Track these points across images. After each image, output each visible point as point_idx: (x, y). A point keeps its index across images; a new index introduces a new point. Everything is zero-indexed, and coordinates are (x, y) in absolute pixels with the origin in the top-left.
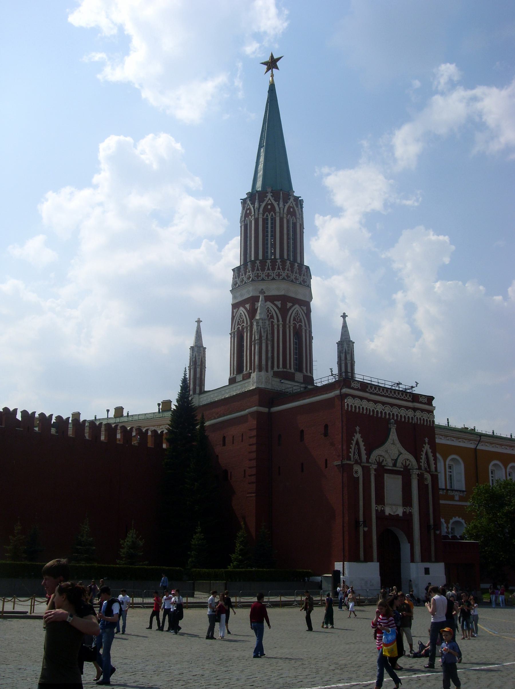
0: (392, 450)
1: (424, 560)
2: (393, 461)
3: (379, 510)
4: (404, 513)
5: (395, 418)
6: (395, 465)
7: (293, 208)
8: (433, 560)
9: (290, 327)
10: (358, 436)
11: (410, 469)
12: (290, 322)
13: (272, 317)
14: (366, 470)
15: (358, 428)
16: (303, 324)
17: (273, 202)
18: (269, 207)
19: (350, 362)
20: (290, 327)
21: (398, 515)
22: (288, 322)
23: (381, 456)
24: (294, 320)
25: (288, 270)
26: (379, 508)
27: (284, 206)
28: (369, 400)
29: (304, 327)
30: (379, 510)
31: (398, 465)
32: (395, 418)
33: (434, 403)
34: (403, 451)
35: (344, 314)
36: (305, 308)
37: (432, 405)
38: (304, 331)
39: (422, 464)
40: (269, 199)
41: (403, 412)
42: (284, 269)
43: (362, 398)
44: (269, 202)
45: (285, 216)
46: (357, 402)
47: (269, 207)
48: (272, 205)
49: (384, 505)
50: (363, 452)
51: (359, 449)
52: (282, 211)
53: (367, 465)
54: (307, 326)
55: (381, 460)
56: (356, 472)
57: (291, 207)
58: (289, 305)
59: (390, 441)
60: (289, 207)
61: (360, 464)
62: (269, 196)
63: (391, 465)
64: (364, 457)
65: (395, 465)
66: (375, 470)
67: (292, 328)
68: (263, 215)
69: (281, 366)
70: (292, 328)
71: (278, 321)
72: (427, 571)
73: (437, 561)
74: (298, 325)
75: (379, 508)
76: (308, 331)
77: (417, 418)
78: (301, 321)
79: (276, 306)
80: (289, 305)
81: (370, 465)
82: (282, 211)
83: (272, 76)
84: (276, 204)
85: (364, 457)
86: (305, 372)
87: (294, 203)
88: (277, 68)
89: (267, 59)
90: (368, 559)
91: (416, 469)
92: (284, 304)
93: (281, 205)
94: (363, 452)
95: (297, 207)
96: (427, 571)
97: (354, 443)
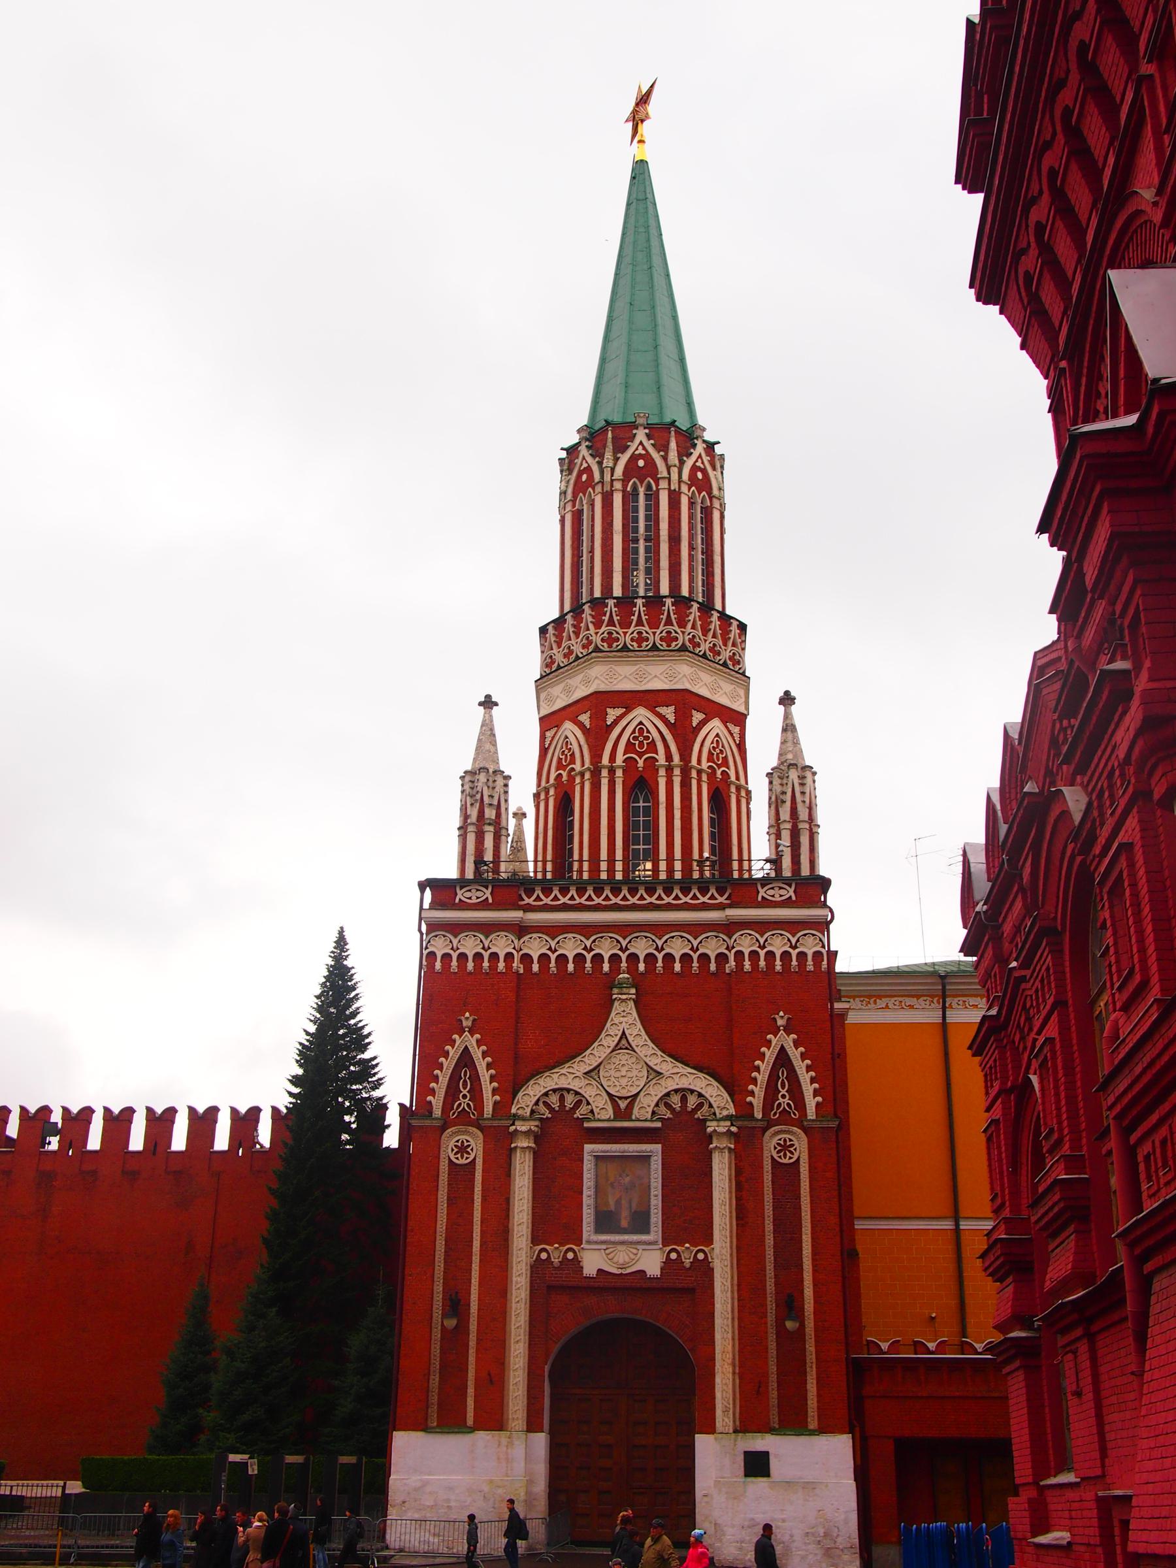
0: (625, 1068)
1: (748, 1423)
2: (623, 1105)
4: (667, 1263)
5: (642, 967)
6: (622, 1114)
7: (647, 456)
8: (813, 1424)
9: (612, 771)
10: (471, 1041)
11: (705, 1120)
17: (589, 459)
18: (584, 477)
19: (789, 826)
20: (612, 771)
21: (644, 1272)
22: (605, 760)
23: (568, 1090)
24: (630, 747)
25: (611, 622)
26: (555, 1253)
27: (616, 460)
28: (521, 930)
30: (556, 1261)
31: (636, 1112)
32: (642, 967)
33: (832, 898)
34: (667, 1065)
35: (787, 693)
36: (669, 712)
37: (824, 905)
38: (662, 772)
39: (757, 1101)
40: (584, 458)
42: (682, 624)
43: (487, 929)
44: (585, 465)
45: (618, 485)
47: (584, 477)
48: (588, 470)
49: (579, 1242)
50: (487, 1087)
51: (475, 1078)
53: (496, 1123)
56: (462, 1149)
57: (640, 456)
58: (612, 714)
59: (608, 1040)
60: (634, 458)
62: (584, 451)
63: (610, 1113)
64: (489, 1100)
65: (626, 1114)
66: (537, 1138)
67: (619, 773)
68: (574, 506)
70: (619, 773)
71: (583, 765)
72: (757, 1465)
74: (641, 763)
75: (555, 1253)
76: (677, 772)
77: (739, 955)
78: (652, 747)
79: (581, 725)
80: (612, 714)
82: (607, 478)
85: (489, 1100)
87: (648, 444)
90: (492, 1419)
91: (728, 1118)
92: (599, 715)
93: (608, 461)
95: (663, 447)
97: (448, 1064)
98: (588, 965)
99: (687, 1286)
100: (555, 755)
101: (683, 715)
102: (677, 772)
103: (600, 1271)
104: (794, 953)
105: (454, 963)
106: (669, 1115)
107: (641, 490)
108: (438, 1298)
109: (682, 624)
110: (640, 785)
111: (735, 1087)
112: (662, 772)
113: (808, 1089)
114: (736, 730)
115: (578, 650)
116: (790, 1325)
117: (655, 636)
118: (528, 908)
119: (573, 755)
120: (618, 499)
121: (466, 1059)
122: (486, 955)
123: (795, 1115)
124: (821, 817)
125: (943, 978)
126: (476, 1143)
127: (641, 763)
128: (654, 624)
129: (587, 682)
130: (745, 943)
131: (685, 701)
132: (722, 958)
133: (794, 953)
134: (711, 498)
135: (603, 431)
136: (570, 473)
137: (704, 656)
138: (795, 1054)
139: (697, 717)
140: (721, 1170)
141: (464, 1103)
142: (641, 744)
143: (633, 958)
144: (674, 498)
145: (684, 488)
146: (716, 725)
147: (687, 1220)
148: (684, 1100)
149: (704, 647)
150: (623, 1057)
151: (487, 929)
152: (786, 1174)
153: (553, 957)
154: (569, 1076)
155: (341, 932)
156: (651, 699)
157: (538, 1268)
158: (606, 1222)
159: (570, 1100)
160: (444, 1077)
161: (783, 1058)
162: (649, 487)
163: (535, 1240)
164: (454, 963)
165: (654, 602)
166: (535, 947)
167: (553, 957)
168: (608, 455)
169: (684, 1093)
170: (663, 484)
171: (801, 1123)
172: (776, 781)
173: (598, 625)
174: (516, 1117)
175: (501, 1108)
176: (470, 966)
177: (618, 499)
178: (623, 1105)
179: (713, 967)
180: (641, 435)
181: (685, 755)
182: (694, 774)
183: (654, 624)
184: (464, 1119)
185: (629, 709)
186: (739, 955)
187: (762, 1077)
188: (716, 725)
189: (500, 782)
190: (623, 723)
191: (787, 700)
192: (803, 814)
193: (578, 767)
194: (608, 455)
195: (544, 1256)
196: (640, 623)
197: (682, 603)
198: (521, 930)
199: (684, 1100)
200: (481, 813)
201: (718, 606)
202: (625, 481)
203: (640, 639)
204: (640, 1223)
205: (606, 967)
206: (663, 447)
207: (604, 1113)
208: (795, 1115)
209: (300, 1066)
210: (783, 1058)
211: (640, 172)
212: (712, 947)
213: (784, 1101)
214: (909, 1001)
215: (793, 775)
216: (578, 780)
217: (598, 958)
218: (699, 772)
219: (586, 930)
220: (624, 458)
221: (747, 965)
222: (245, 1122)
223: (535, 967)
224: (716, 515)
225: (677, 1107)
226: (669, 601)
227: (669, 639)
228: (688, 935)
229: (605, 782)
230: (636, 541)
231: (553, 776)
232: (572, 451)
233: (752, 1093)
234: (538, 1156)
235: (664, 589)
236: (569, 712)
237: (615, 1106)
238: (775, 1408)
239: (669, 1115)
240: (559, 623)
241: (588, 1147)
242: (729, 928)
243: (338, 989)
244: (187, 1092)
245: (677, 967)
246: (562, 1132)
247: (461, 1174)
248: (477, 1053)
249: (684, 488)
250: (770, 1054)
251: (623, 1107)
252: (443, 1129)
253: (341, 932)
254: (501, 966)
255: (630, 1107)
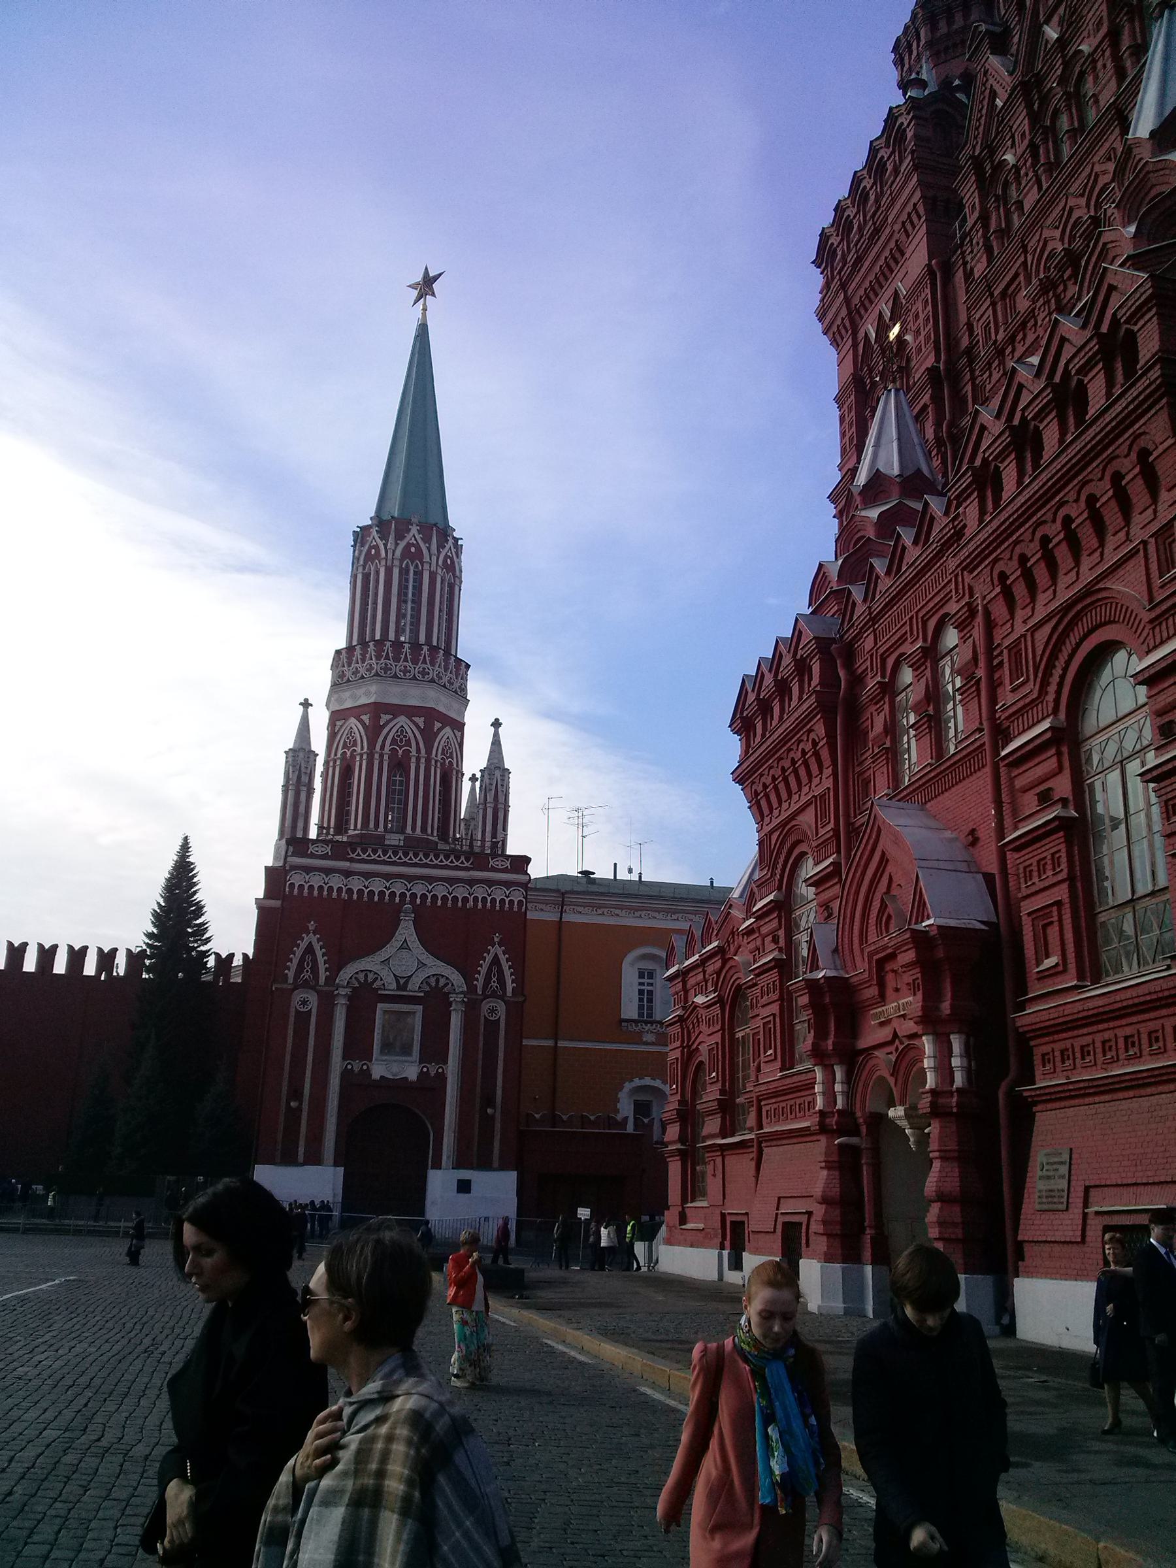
0: (404, 960)
1: (458, 1165)
2: (402, 981)
3: (356, 1070)
5: (418, 901)
6: (402, 986)
7: (417, 546)
8: (496, 1164)
9: (382, 756)
10: (313, 938)
12: (382, 748)
13: (355, 744)
14: (327, 1002)
15: (312, 925)
16: (414, 750)
17: (378, 540)
20: (382, 756)
24: (394, 742)
25: (387, 657)
26: (356, 1066)
27: (397, 544)
28: (347, 874)
29: (414, 753)
30: (356, 1070)
31: (409, 987)
32: (418, 901)
35: (497, 720)
36: (420, 721)
38: (413, 760)
41: (441, 891)
43: (328, 871)
45: (397, 563)
46: (316, 880)
48: (377, 547)
50: (322, 967)
52: (390, 555)
54: (423, 751)
55: (370, 980)
56: (304, 1003)
57: (413, 545)
58: (385, 718)
59: (396, 942)
60: (409, 545)
61: (313, 988)
63: (394, 986)
64: (323, 975)
65: (403, 987)
67: (386, 757)
69: (359, 826)
70: (386, 757)
71: (362, 748)
72: (464, 1187)
73: (503, 1167)
74: (400, 752)
75: (356, 1066)
76: (423, 760)
77: (476, 899)
78: (408, 743)
80: (385, 718)
81: (332, 989)
82: (390, 555)
83: (425, 309)
84: (382, 547)
85: (323, 975)
86: (409, 830)
88: (433, 295)
89: (419, 278)
90: (314, 1159)
91: (461, 993)
92: (376, 718)
94: (322, 967)
95: (427, 540)
96: (464, 1187)
97: (299, 952)
98: (387, 897)
99: (431, 1087)
100: (341, 739)
101: (429, 724)
102: (423, 760)
103: (382, 1077)
104: (507, 900)
105: (306, 890)
106: (428, 989)
107: (412, 568)
108: (285, 1089)
109: (433, 664)
110: (399, 765)
111: (468, 976)
112: (413, 760)
113: (509, 979)
114: (458, 734)
115: (362, 671)
116: (489, 1111)
117: (415, 670)
118: (352, 860)
119: (355, 741)
120: (396, 571)
121: (310, 949)
122: (326, 888)
123: (500, 993)
124: (513, 800)
125: (563, 894)
126: (313, 999)
127: (400, 752)
128: (415, 662)
129: (368, 694)
130: (480, 892)
131: (430, 714)
132: (465, 900)
133: (507, 900)
134: (455, 576)
135: (389, 522)
136: (362, 545)
137: (444, 686)
138: (503, 959)
139: (438, 725)
140: (456, 1021)
141: (307, 975)
142: (401, 740)
143: (414, 896)
144: (433, 576)
145: (439, 571)
146: (448, 729)
147: (434, 1050)
148: (437, 981)
149: (445, 680)
150: (404, 953)
151: (328, 871)
152: (493, 1025)
153: (366, 891)
154: (370, 963)
155: (186, 839)
156: (410, 712)
157: (346, 1074)
158: (387, 1047)
159: (371, 977)
160: (296, 961)
161: (496, 961)
162: (417, 566)
163: (344, 1058)
164: (306, 890)
165: (416, 646)
166: (356, 884)
167: (366, 891)
168: (391, 540)
169: (438, 977)
170: (426, 566)
171: (502, 997)
172: (486, 776)
173: (378, 658)
174: (338, 987)
175: (330, 980)
176: (316, 893)
177: (396, 571)
178: (402, 981)
179: (460, 904)
180: (414, 530)
181: (429, 752)
182: (433, 762)
183: (415, 662)
184: (306, 985)
185: (395, 717)
186: (476, 899)
187: (483, 970)
188: (448, 729)
189: (312, 757)
190: (391, 725)
191: (497, 724)
192: (501, 799)
193: (358, 749)
194: (391, 540)
195: (349, 1067)
196: (406, 660)
197: (434, 650)
198: (347, 874)
199: (437, 981)
200: (299, 778)
201: (453, 653)
202: (401, 561)
203: (405, 671)
204: (406, 1050)
205: (397, 900)
206: (427, 540)
207: (391, 985)
208: (500, 993)
209: (155, 926)
210: (496, 961)
211: (423, 333)
212: (460, 892)
213: (494, 984)
214: (541, 906)
215: (498, 773)
216: (358, 758)
217: (393, 894)
218: (436, 761)
219: (387, 876)
220: (402, 544)
221: (480, 905)
222: (106, 959)
223: (355, 897)
224: (457, 588)
225: (433, 984)
226: (425, 648)
227: (424, 673)
228: (442, 883)
229: (376, 763)
230: (406, 602)
231: (340, 752)
232: (365, 529)
233: (477, 980)
234: (350, 1010)
235: (422, 639)
236: (356, 712)
237: (398, 982)
238: (475, 1155)
239: (428, 989)
240: (350, 649)
241: (379, 1005)
242: (471, 882)
243: (182, 879)
244: (63, 934)
245: (439, 903)
246: (365, 996)
247: (303, 1018)
248: (317, 947)
249: (439, 571)
250: (489, 958)
251: (402, 986)
252: (293, 990)
253: (186, 839)
254: (335, 895)
255: (406, 983)
